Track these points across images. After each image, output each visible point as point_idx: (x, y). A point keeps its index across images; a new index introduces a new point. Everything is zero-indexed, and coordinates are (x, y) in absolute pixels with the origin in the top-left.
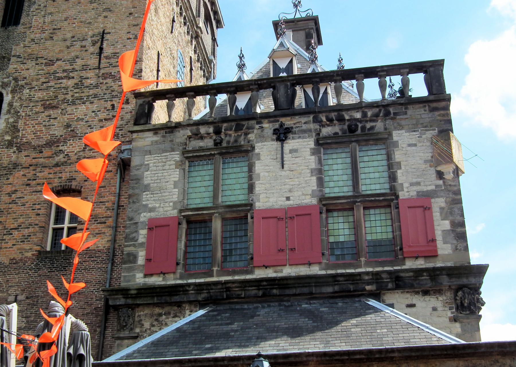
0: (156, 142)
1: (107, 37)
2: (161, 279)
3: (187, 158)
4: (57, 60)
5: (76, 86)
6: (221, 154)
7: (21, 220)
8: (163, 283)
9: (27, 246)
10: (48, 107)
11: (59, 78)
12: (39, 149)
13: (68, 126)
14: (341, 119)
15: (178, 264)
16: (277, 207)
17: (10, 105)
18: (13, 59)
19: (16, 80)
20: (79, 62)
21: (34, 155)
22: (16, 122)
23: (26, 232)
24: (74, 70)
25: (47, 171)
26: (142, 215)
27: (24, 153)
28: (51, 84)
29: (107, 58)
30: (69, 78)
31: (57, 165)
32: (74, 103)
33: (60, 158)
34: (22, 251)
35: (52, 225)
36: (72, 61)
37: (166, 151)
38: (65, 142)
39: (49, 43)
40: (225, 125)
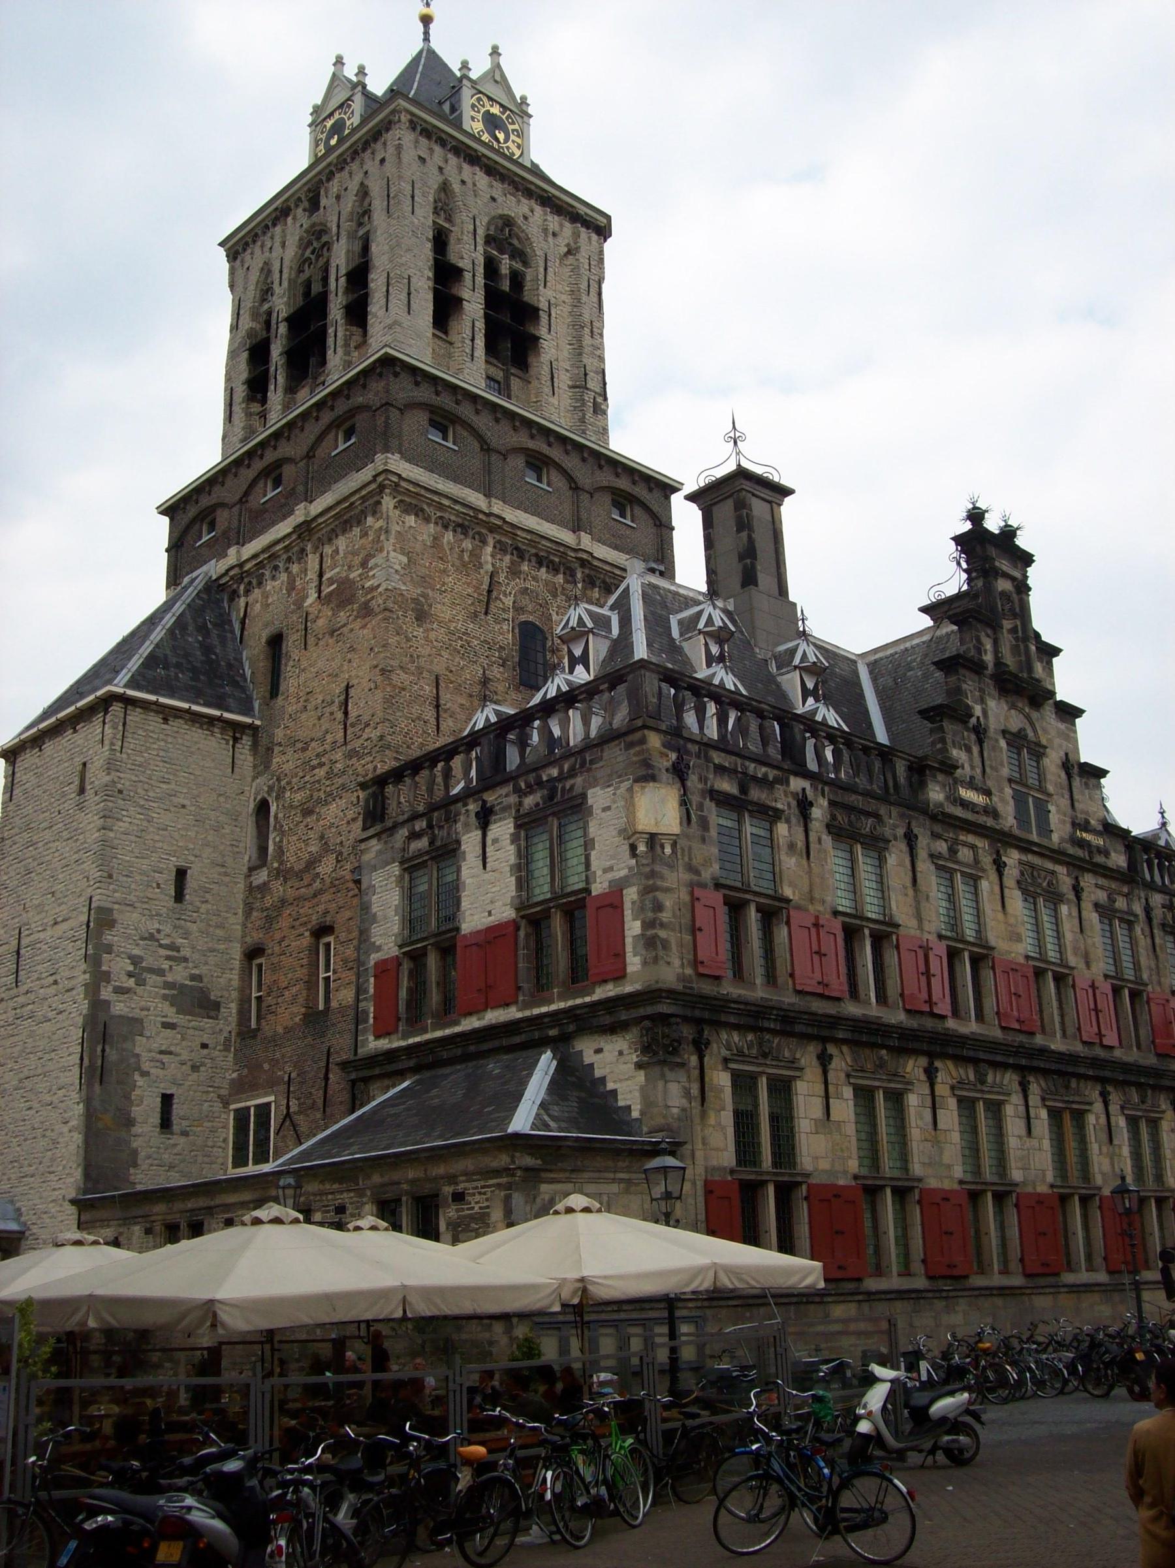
0: (380, 852)
1: (352, 692)
2: (387, 1041)
3: (405, 870)
4: (312, 740)
5: (329, 775)
6: (432, 859)
7: (290, 976)
8: (389, 1046)
9: (295, 1009)
10: (307, 812)
11: (314, 768)
12: (299, 875)
13: (322, 837)
14: (540, 783)
15: (399, 1019)
16: (480, 927)
17: (276, 817)
18: (277, 749)
19: (279, 780)
20: (329, 738)
21: (297, 885)
22: (281, 841)
23: (294, 990)
24: (325, 752)
25: (307, 904)
26: (373, 956)
27: (289, 884)
28: (307, 778)
29: (353, 725)
30: (321, 765)
31: (315, 896)
32: (327, 803)
33: (317, 885)
34: (293, 1015)
35: (322, 975)
36: (323, 740)
37: (388, 864)
38: (320, 861)
39: (304, 716)
40: (436, 814)
